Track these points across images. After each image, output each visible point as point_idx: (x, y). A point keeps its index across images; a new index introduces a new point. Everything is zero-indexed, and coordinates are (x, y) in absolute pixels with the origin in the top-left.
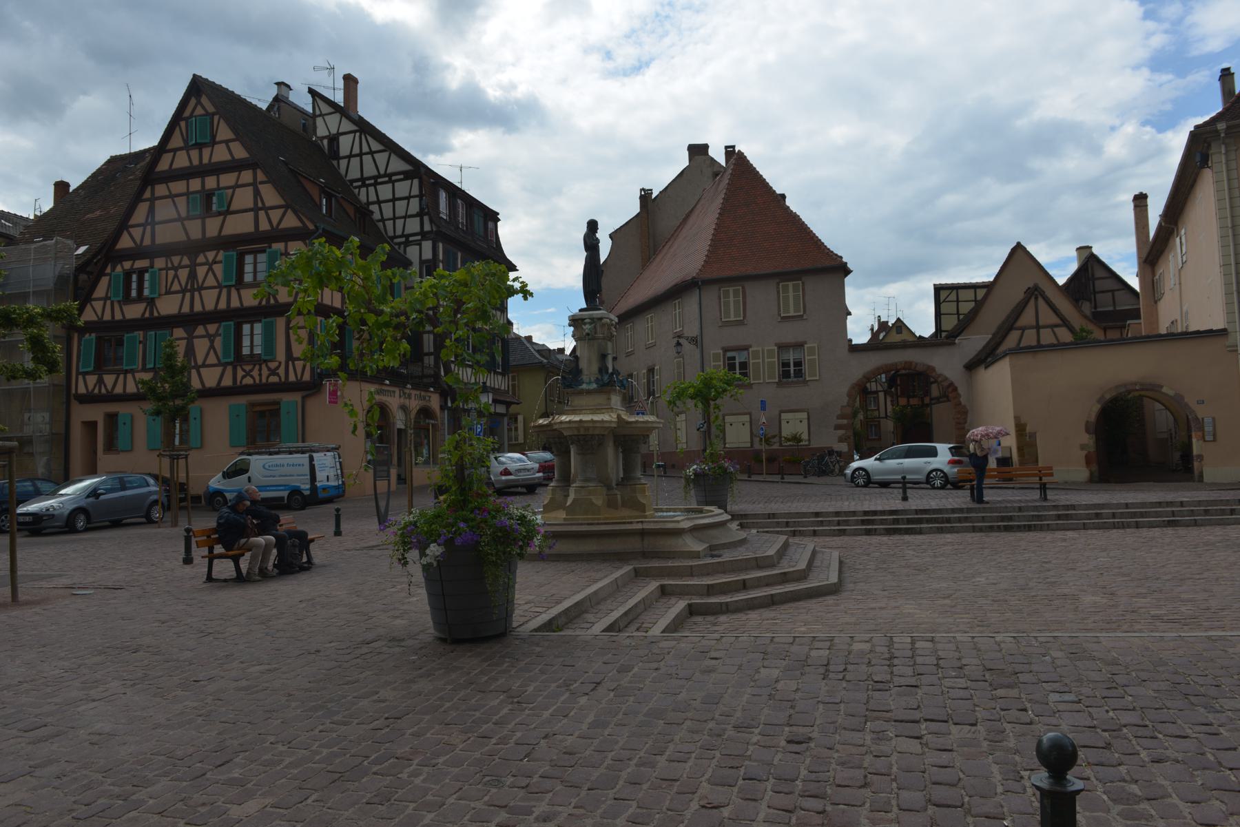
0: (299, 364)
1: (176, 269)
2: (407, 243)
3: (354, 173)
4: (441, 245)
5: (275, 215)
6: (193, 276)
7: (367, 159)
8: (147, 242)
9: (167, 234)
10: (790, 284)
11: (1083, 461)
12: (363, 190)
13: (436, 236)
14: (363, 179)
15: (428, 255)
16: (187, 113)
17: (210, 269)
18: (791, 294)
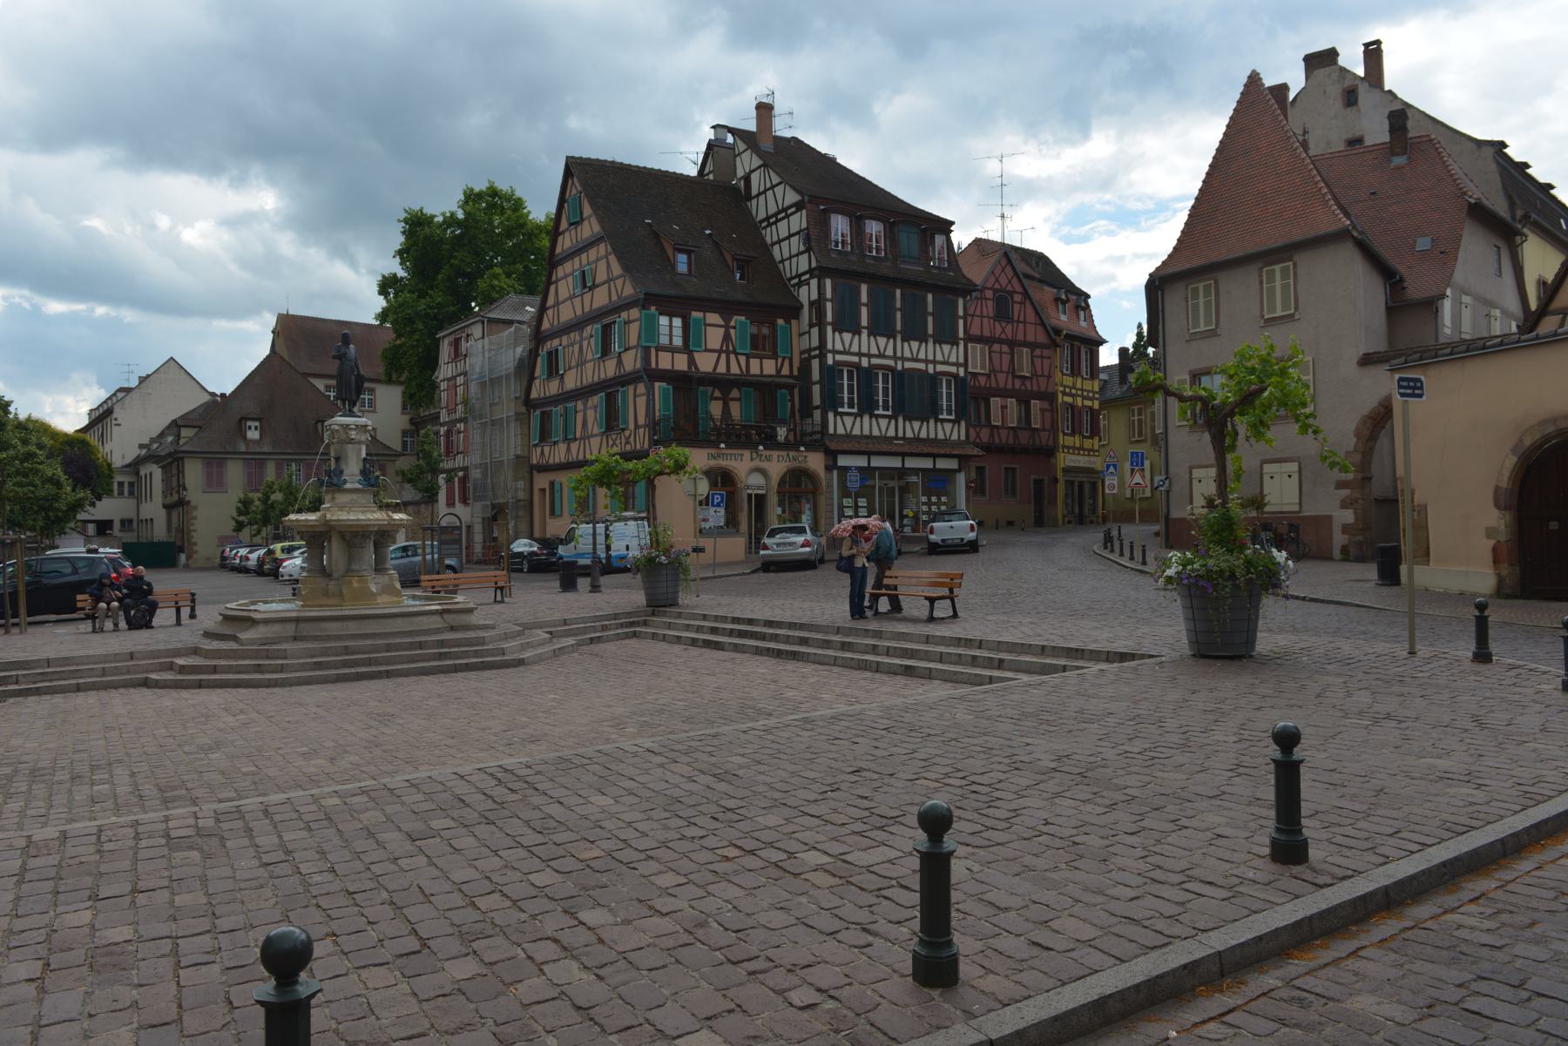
1: (572, 345)
2: (800, 284)
3: (762, 215)
4: (828, 282)
5: (619, 282)
7: (770, 193)
10: (1277, 268)
11: (1489, 557)
13: (819, 272)
14: (767, 218)
15: (814, 296)
18: (1278, 283)
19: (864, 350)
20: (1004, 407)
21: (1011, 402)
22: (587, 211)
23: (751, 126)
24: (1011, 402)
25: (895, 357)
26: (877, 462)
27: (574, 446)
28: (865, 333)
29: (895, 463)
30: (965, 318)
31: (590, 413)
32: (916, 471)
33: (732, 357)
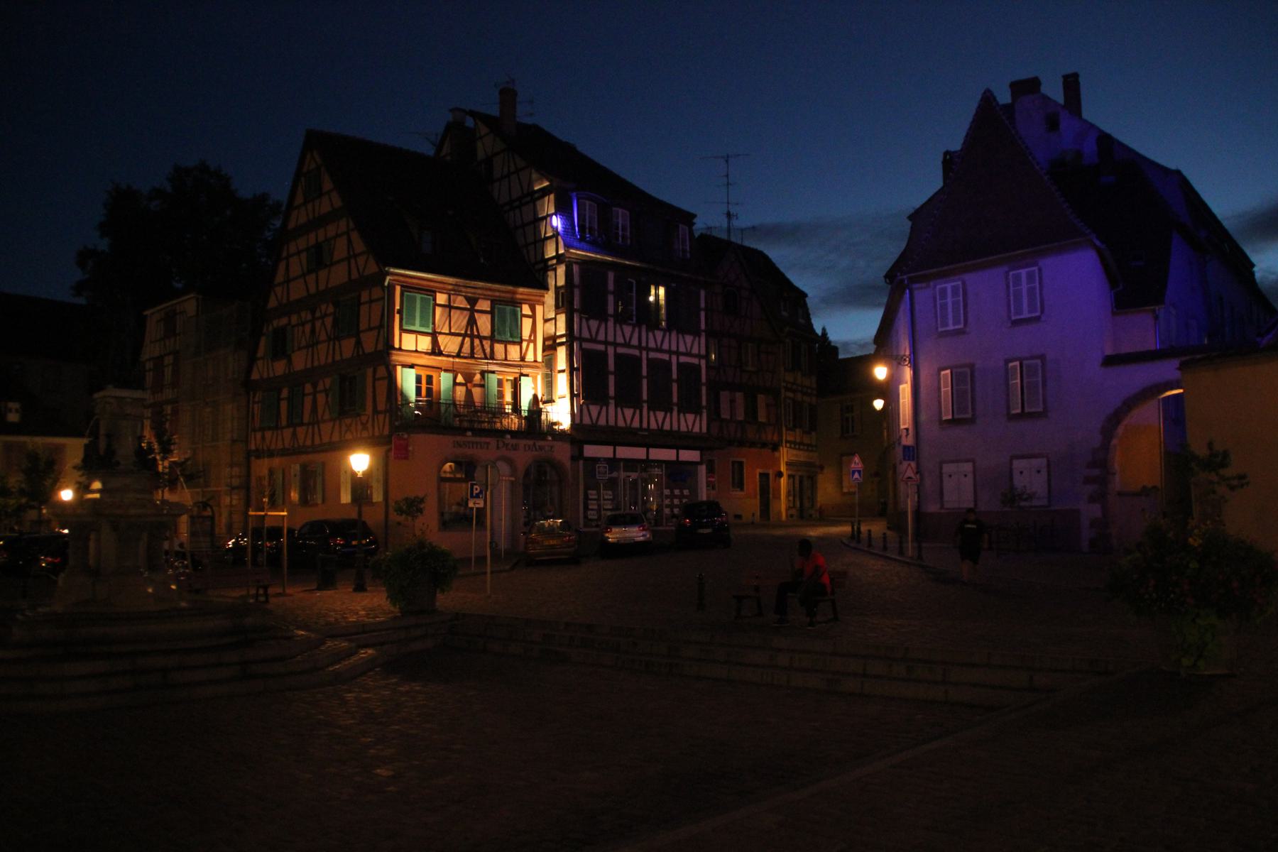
0: (381, 417)
1: (303, 324)
5: (361, 260)
6: (313, 331)
8: (285, 301)
9: (297, 291)
12: (511, 213)
16: (305, 170)
17: (323, 323)
19: (611, 339)
20: (732, 401)
21: (739, 396)
22: (328, 184)
23: (494, 111)
24: (739, 396)
25: (639, 347)
26: (624, 452)
27: (301, 431)
28: (611, 324)
29: (638, 453)
30: (706, 310)
31: (321, 398)
32: (659, 463)
33: (477, 342)
